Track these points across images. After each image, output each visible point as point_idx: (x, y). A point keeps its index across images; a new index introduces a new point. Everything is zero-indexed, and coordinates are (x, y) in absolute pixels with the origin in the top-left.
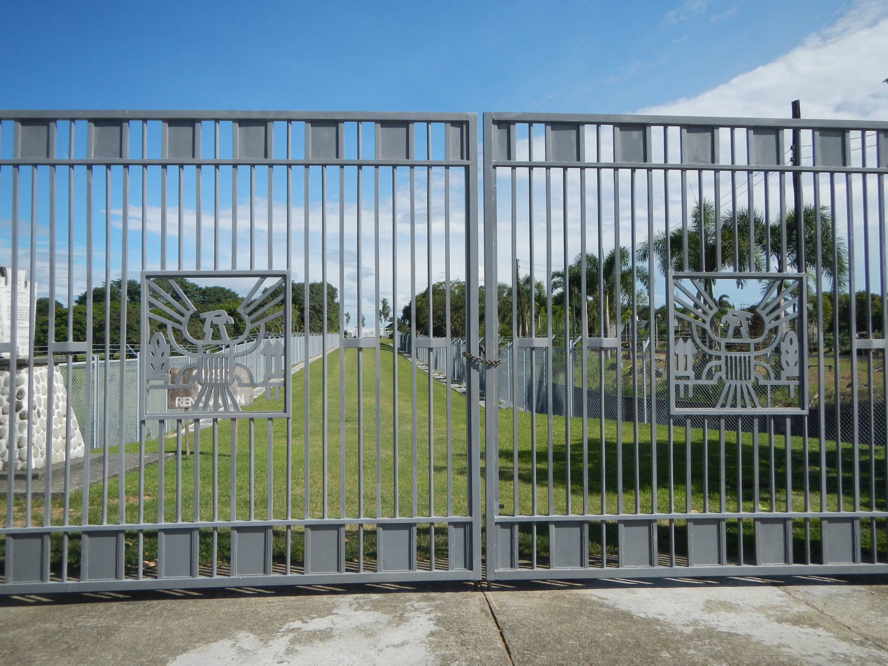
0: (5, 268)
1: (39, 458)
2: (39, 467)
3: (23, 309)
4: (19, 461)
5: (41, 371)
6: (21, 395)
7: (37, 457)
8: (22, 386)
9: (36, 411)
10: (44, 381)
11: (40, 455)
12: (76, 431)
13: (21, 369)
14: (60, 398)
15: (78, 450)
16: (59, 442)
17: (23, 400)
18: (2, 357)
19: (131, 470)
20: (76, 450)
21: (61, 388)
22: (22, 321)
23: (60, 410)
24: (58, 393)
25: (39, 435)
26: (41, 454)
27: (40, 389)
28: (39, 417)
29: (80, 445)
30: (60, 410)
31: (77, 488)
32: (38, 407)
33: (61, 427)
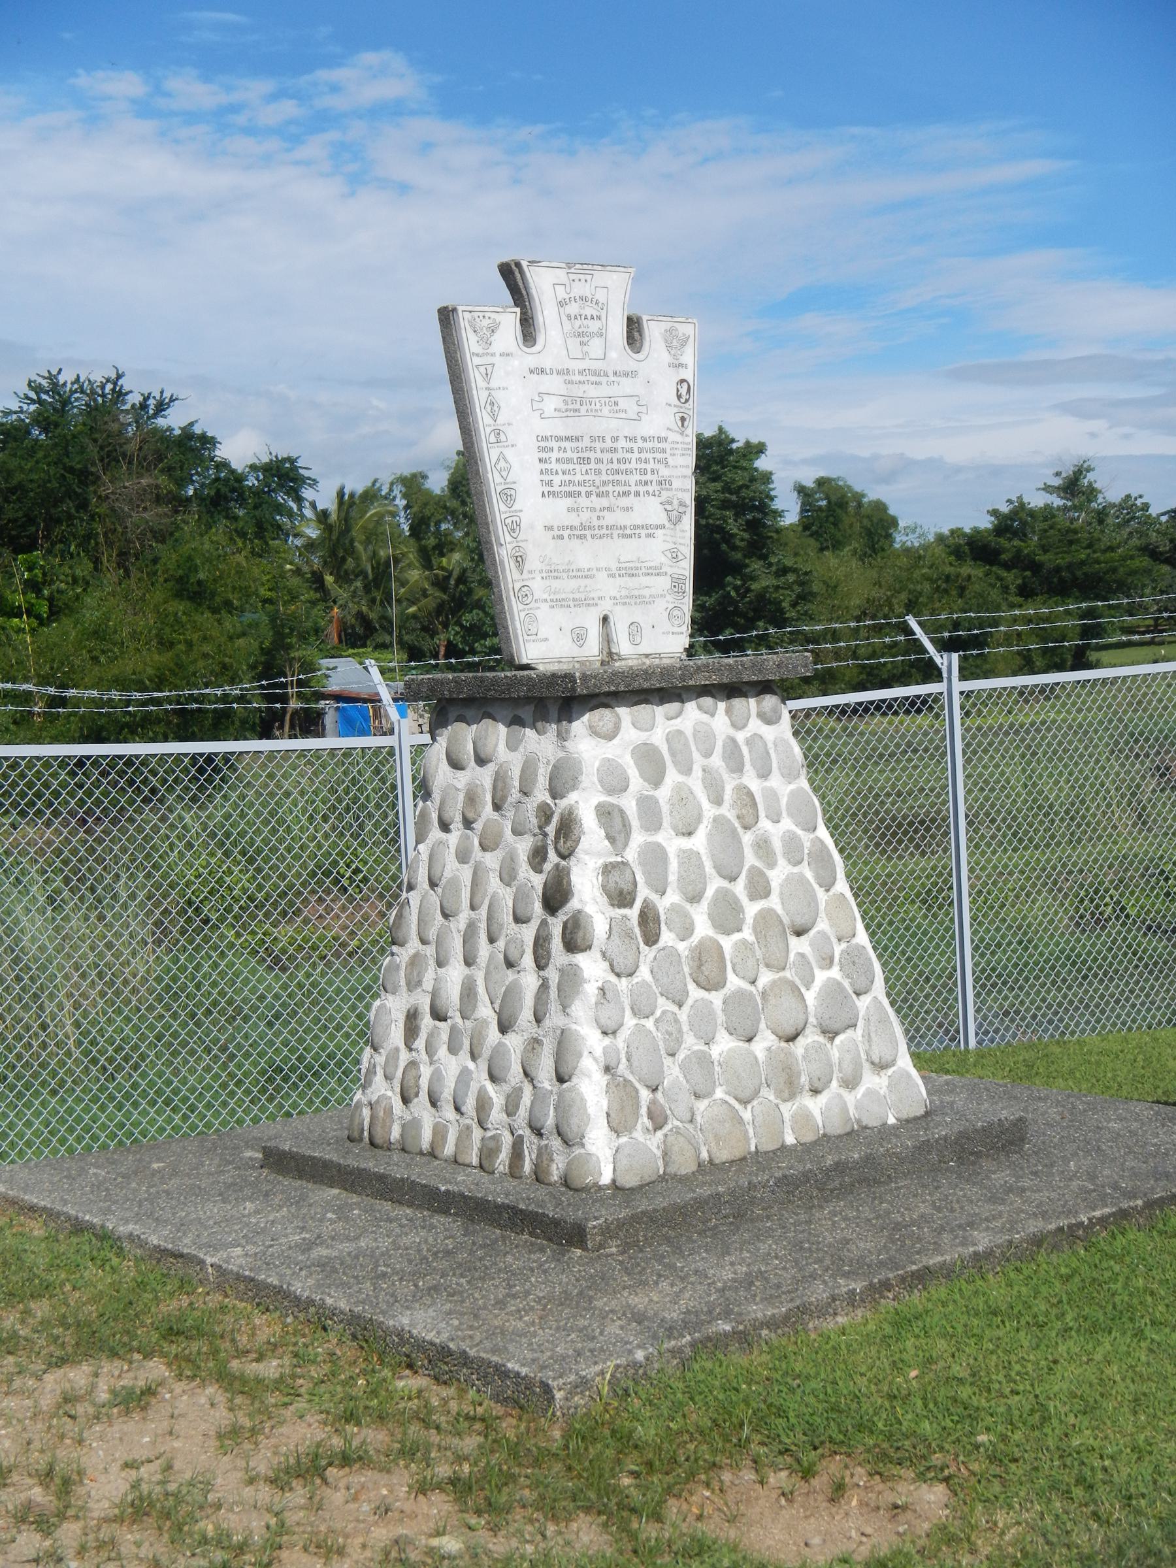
0: (518, 265)
1: (638, 1134)
2: (629, 1181)
3: (622, 443)
4: (556, 1143)
5: (677, 724)
6: (566, 837)
7: (630, 1129)
8: (572, 797)
9: (633, 913)
10: (687, 771)
11: (644, 1120)
12: (863, 1004)
13: (570, 721)
14: (777, 845)
15: (869, 1093)
16: (761, 1055)
17: (573, 861)
18: (527, 667)
19: (1037, 1241)
20: (861, 1091)
21: (784, 801)
22: (624, 502)
23: (774, 902)
24: (765, 824)
25: (649, 1024)
26: (650, 1116)
27: (665, 808)
28: (651, 938)
29: (880, 1066)
30: (774, 902)
31: (640, 1355)
32: (643, 893)
33: (774, 983)
